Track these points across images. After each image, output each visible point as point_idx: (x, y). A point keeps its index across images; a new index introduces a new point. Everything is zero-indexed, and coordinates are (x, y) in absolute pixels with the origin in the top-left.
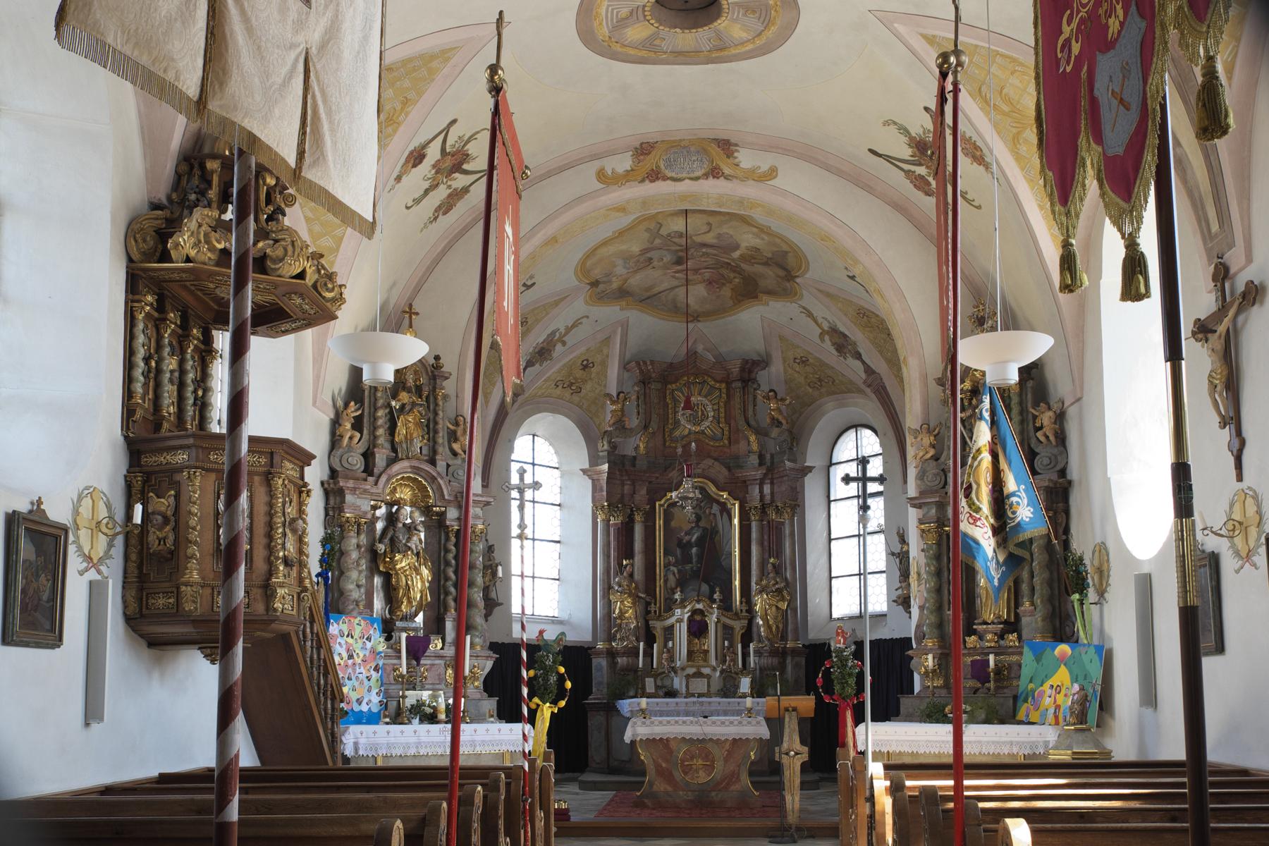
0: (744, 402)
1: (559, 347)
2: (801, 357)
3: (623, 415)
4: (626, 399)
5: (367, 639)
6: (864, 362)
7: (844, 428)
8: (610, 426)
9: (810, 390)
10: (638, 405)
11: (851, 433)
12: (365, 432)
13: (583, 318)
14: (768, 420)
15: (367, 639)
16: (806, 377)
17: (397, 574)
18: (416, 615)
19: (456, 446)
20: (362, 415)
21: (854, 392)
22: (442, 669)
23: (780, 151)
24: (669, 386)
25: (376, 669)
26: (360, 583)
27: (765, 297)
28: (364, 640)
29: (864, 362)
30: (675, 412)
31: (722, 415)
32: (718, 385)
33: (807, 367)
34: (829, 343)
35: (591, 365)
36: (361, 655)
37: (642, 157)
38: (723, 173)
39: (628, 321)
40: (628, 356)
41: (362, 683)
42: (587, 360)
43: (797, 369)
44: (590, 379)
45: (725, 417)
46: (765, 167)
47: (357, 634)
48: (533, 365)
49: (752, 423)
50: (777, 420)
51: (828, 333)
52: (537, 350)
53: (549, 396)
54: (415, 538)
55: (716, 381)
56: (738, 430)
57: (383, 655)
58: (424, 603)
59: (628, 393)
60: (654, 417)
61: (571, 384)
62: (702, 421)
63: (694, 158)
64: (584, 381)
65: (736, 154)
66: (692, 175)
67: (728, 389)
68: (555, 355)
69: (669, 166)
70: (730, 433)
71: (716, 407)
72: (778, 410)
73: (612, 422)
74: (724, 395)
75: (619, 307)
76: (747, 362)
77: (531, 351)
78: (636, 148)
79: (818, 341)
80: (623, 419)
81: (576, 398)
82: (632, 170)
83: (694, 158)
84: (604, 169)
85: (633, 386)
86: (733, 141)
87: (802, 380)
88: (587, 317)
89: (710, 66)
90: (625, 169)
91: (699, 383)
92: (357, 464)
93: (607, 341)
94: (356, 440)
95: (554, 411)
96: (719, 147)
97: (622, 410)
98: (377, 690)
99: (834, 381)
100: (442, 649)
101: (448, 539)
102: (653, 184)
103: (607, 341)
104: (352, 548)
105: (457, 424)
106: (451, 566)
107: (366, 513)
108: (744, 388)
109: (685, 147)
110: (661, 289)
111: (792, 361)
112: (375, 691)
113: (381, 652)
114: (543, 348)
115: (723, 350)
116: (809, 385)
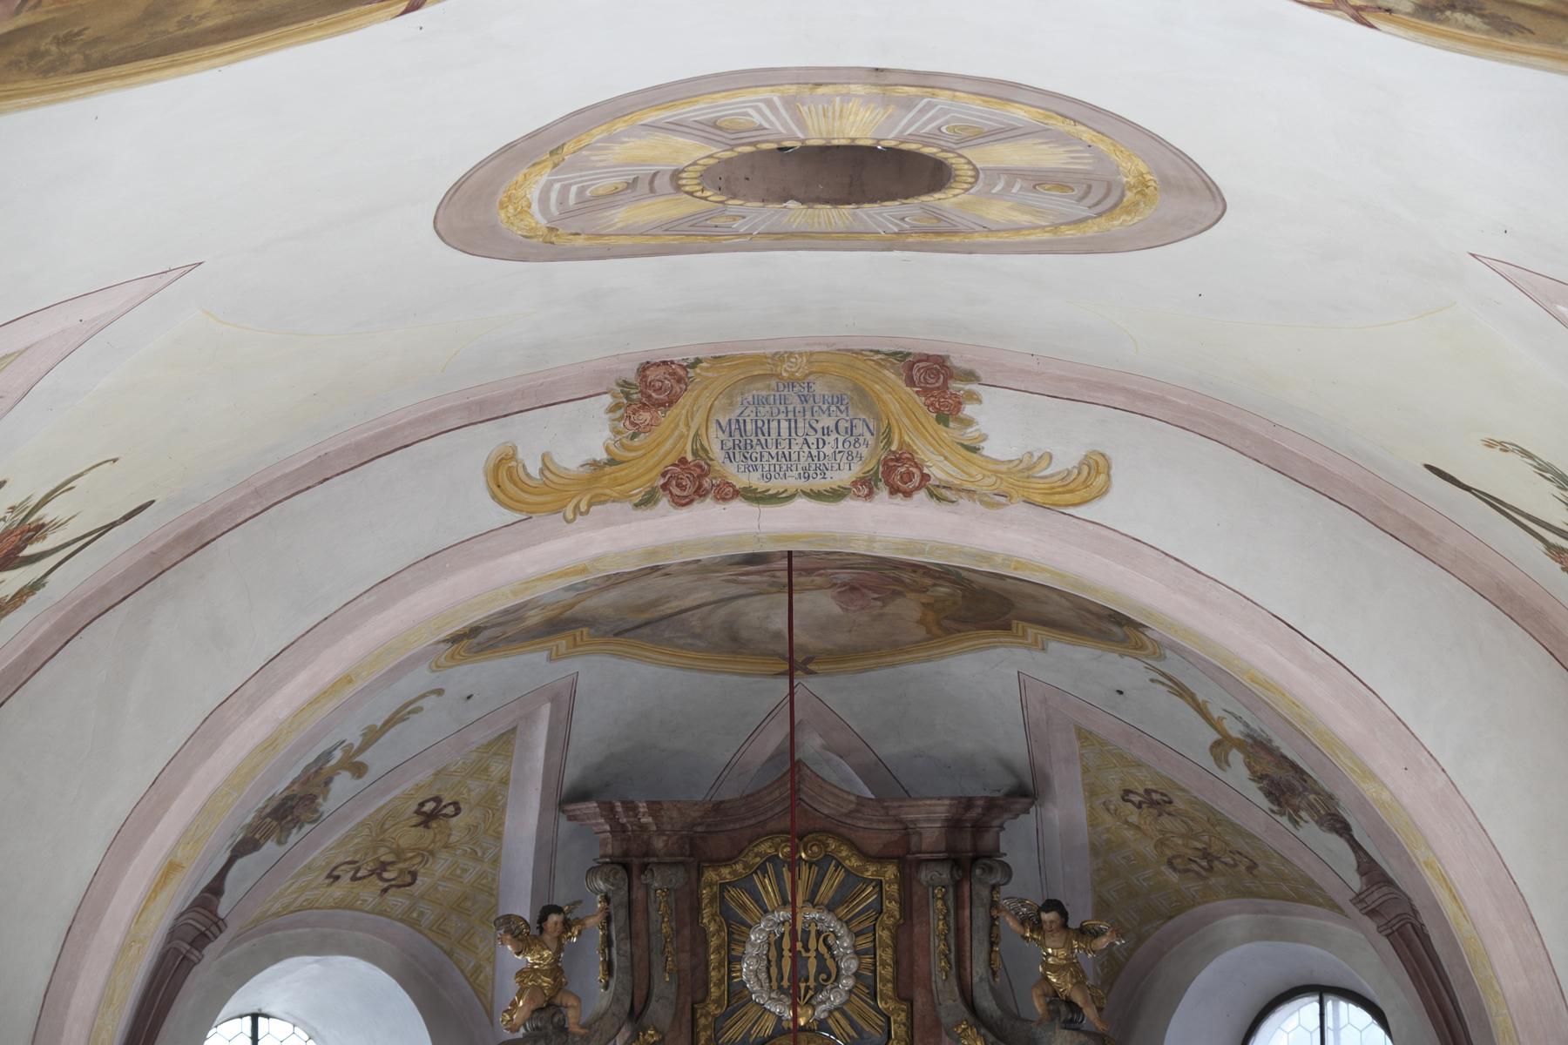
0: (959, 931)
1: (343, 785)
2: (1148, 792)
3: (559, 987)
4: (567, 925)
6: (1356, 846)
7: (1282, 988)
9: (1174, 877)
10: (608, 942)
11: (1307, 1009)
13: (423, 696)
14: (1039, 1005)
16: (1161, 843)
21: (1319, 905)
23: (1119, 400)
24: (710, 875)
27: (1032, 631)
29: (1356, 846)
30: (733, 960)
31: (886, 972)
32: (870, 871)
33: (1165, 819)
34: (1244, 772)
35: (450, 810)
37: (645, 416)
38: (925, 477)
39: (574, 683)
40: (572, 774)
42: (437, 800)
43: (1134, 819)
44: (446, 846)
45: (896, 980)
46: (1067, 458)
49: (986, 1002)
50: (1070, 1003)
51: (1239, 745)
53: (311, 906)
55: (867, 857)
56: (937, 1022)
59: (574, 904)
60: (663, 984)
61: (384, 866)
62: (819, 988)
63: (827, 422)
64: (427, 854)
65: (969, 410)
66: (818, 484)
67: (906, 882)
68: (328, 805)
69: (740, 449)
70: (910, 1025)
71: (864, 943)
72: (1071, 966)
74: (892, 906)
75: (545, 654)
76: (969, 803)
77: (248, 820)
78: (626, 384)
79: (1208, 762)
80: (557, 1001)
81: (397, 900)
82: (612, 462)
83: (827, 422)
84: (513, 457)
85: (592, 871)
86: (956, 362)
87: (1148, 848)
88: (439, 692)
89: (896, 254)
90: (585, 458)
91: (811, 864)
93: (505, 742)
95: (321, 947)
96: (910, 382)
97: (556, 970)
99: (1252, 867)
102: (684, 513)
103: (505, 742)
108: (957, 885)
109: (791, 383)
110: (687, 603)
111: (1116, 798)
115: (888, 749)
116: (1170, 863)
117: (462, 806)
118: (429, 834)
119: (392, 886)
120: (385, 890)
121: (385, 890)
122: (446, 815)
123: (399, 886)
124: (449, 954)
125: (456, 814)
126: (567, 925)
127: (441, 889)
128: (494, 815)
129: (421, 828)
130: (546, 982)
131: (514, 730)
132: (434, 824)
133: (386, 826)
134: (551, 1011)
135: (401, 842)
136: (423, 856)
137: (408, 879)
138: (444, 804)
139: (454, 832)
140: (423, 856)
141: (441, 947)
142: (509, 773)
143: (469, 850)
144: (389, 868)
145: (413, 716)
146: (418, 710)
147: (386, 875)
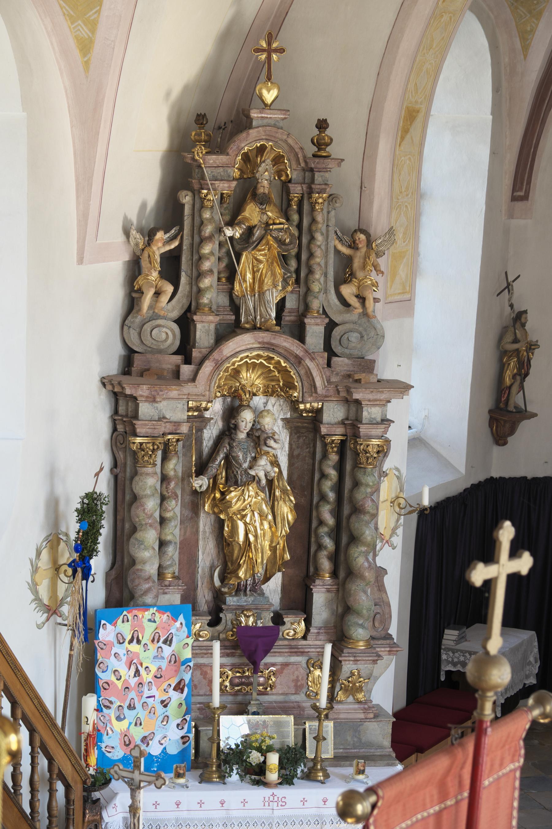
5: (165, 642)
12: (184, 279)
15: (165, 642)
17: (231, 519)
18: (267, 579)
19: (348, 291)
20: (179, 248)
22: (302, 672)
25: (179, 688)
26: (169, 538)
28: (160, 644)
36: (153, 669)
41: (152, 711)
47: (146, 638)
54: (263, 462)
57: (191, 664)
58: (279, 562)
92: (166, 340)
94: (165, 299)
98: (179, 721)
100: (304, 638)
101: (325, 456)
104: (148, 492)
105: (353, 246)
106: (328, 503)
107: (177, 424)
112: (175, 721)
113: (189, 660)
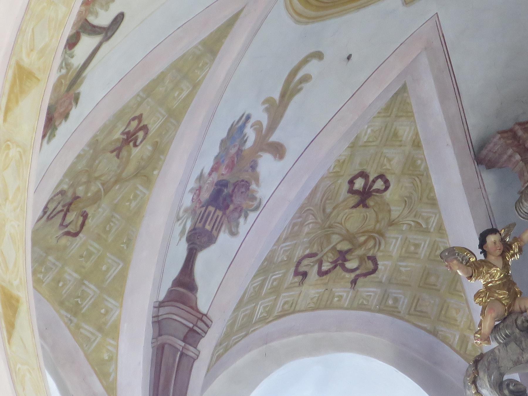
4: (507, 247)
8: (487, 340)
13: (305, 61)
39: (438, 27)
42: (363, 175)
44: (391, 223)
48: (211, 239)
52: (205, 196)
73: (488, 326)
88: (319, 55)
114: (221, 185)
117: (389, 177)
118: (370, 213)
119: (358, 276)
120: (354, 282)
121: (354, 282)
122: (378, 191)
123: (365, 275)
124: (434, 333)
125: (387, 188)
126: (507, 247)
127: (403, 269)
128: (421, 181)
129: (360, 209)
130: (502, 294)
131: (404, 88)
132: (371, 202)
133: (328, 210)
134: (514, 317)
135: (348, 225)
136: (374, 238)
137: (370, 265)
138: (371, 179)
139: (393, 208)
140: (374, 238)
141: (425, 329)
142: (417, 134)
143: (413, 223)
144: (348, 257)
145: (306, 86)
146: (306, 78)
147: (350, 265)
